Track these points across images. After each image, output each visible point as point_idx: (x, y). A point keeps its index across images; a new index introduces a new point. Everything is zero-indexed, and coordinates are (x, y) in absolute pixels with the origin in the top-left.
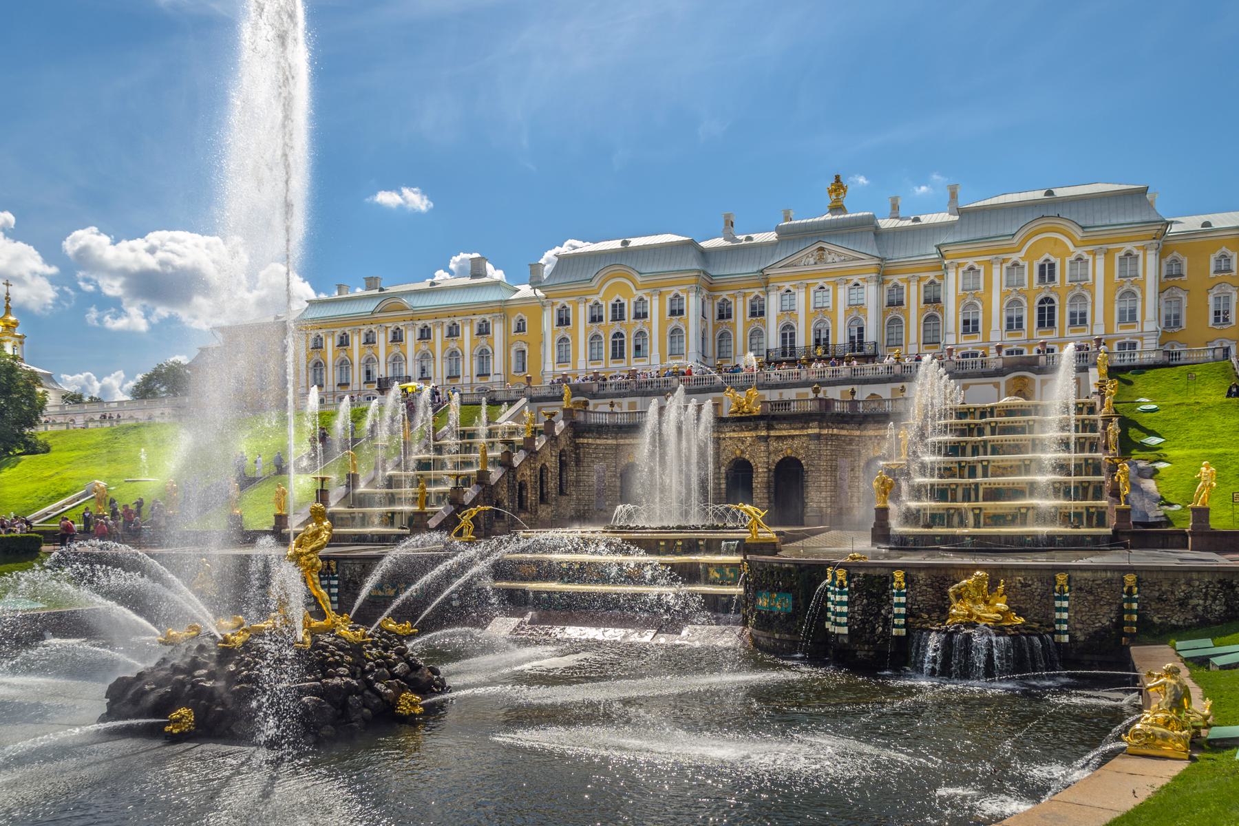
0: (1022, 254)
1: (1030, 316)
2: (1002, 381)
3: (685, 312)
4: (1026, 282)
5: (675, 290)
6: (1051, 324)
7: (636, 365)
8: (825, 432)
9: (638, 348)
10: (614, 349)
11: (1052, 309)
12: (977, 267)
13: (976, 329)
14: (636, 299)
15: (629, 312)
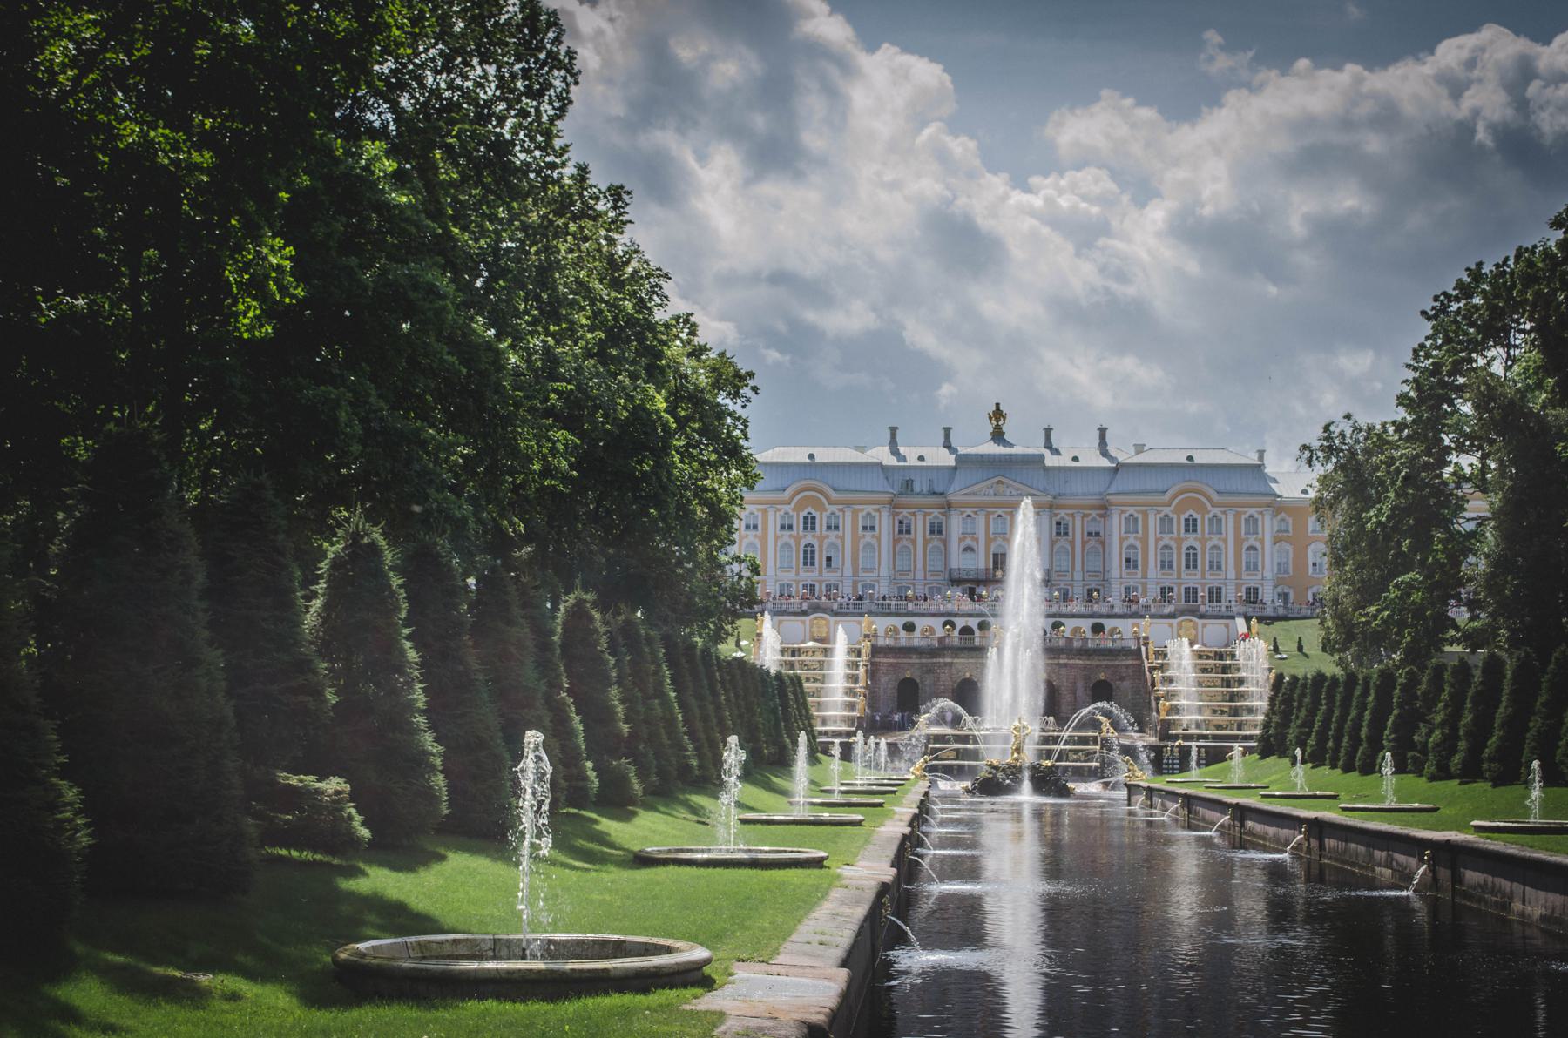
0: (1172, 508)
1: (1179, 560)
2: (1174, 622)
3: (877, 528)
4: (1175, 531)
5: (869, 508)
6: (1195, 566)
7: (830, 576)
8: (1071, 662)
9: (829, 559)
10: (805, 558)
11: (1195, 555)
12: (1136, 515)
13: (1136, 567)
14: (829, 512)
15: (821, 523)
